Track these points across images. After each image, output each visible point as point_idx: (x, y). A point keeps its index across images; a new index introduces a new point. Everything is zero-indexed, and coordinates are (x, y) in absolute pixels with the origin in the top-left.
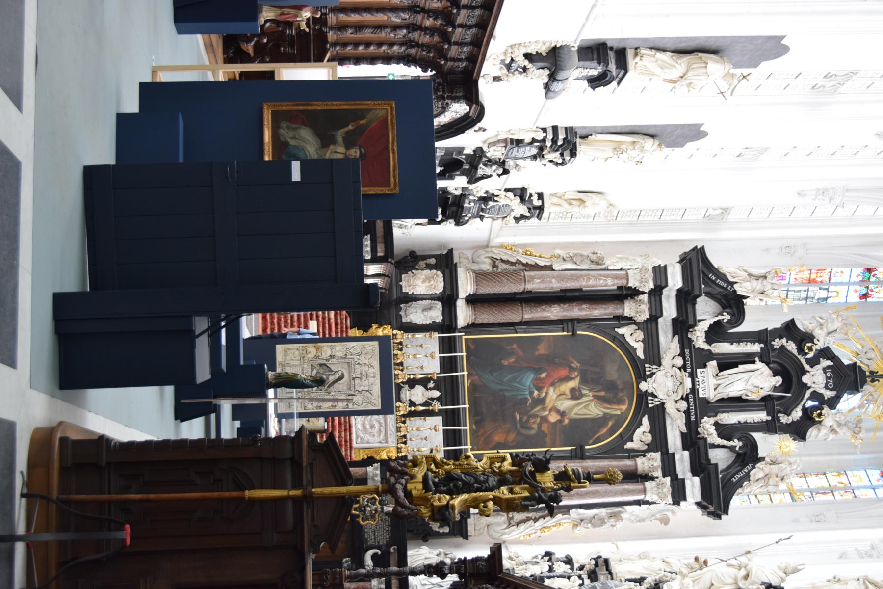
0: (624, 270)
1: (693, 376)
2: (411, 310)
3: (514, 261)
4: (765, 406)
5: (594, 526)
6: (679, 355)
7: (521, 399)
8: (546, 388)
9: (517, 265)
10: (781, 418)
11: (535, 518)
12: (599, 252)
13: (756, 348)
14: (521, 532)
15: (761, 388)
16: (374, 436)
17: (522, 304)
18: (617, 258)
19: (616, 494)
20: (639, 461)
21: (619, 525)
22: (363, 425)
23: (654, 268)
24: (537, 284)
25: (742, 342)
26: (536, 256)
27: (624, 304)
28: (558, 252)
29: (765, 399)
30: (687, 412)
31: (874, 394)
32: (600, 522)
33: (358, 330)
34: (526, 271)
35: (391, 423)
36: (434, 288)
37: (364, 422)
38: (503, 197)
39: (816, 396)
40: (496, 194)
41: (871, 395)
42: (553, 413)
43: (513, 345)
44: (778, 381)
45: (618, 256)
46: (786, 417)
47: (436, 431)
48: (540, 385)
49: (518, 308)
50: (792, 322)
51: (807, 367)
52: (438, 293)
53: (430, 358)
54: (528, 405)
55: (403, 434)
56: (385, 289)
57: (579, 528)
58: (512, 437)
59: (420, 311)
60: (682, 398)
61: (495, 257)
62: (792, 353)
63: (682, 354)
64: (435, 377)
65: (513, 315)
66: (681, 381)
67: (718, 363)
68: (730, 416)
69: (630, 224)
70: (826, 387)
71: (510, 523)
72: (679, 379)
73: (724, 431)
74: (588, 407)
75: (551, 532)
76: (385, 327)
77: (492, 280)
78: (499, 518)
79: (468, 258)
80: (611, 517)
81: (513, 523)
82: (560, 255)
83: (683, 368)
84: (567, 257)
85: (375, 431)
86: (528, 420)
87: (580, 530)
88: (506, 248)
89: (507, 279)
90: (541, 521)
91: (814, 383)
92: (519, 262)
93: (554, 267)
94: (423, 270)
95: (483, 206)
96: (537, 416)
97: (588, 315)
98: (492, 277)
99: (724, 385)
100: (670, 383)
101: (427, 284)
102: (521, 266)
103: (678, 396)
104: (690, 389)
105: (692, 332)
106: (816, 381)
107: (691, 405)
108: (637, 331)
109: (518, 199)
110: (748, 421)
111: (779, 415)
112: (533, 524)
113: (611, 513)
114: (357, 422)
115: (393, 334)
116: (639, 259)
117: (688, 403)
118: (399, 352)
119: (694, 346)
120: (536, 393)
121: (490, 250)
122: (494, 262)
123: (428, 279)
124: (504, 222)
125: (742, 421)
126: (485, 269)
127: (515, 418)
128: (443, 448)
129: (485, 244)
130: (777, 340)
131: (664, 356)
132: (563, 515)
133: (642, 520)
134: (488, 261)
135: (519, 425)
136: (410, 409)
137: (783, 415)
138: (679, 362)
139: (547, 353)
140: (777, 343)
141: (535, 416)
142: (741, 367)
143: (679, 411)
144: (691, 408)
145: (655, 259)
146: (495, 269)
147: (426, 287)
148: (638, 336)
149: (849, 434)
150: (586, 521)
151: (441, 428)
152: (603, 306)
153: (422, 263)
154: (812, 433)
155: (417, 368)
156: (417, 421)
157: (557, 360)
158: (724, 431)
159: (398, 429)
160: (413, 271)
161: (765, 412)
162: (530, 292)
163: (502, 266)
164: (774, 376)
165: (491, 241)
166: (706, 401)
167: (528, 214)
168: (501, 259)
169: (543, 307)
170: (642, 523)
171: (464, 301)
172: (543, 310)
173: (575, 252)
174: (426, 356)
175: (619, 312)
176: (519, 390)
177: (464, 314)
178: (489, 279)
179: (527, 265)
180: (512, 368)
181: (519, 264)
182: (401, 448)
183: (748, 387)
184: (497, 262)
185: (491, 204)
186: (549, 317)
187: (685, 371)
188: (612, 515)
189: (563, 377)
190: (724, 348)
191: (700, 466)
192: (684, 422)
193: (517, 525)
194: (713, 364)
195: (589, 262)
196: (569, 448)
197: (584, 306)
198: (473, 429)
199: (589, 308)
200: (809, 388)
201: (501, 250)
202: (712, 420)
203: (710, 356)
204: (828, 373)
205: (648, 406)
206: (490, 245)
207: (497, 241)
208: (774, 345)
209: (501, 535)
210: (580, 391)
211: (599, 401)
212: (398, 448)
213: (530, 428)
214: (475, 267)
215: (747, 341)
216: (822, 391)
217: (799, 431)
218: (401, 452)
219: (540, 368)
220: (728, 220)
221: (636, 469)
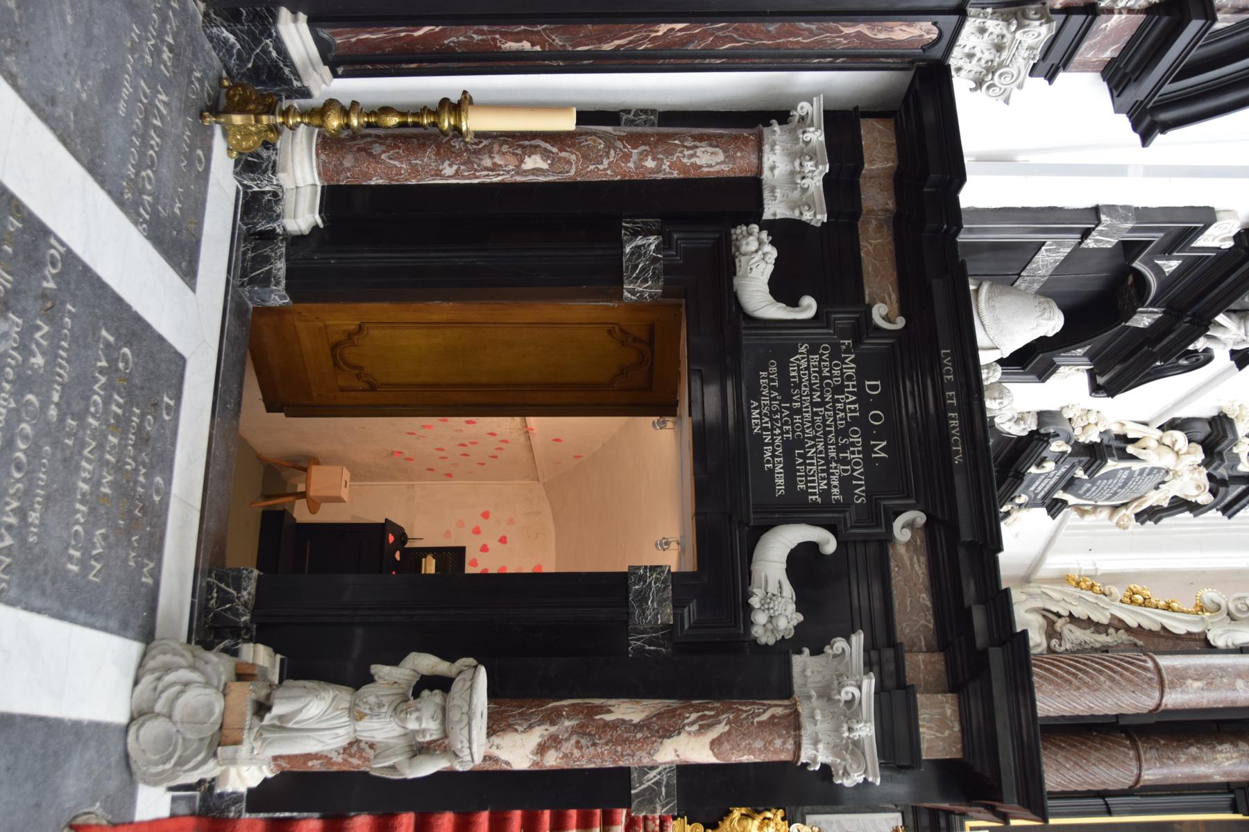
3: (1105, 621)
9: (1111, 630)
17: (1134, 743)
26: (1157, 608)
28: (1209, 595)
33: (690, 823)
38: (1153, 444)
40: (1130, 436)
49: (1126, 755)
61: (1054, 609)
65: (1114, 773)
76: (769, 815)
77: (1071, 683)
82: (1219, 608)
84: (1239, 611)
88: (1078, 584)
89: (1112, 679)
95: (1080, 473)
98: (1068, 672)
102: (1123, 636)
109: (1199, 456)
121: (1038, 591)
122: (1051, 624)
124: (1116, 519)
129: (1022, 572)
146: (1054, 642)
162: (1168, 712)
163: (1074, 636)
167: (1205, 498)
168: (1071, 615)
169: (1193, 750)
172: (1195, 759)
179: (1139, 631)
181: (1117, 630)
184: (1059, 623)
185: (1111, 465)
186: (1210, 776)
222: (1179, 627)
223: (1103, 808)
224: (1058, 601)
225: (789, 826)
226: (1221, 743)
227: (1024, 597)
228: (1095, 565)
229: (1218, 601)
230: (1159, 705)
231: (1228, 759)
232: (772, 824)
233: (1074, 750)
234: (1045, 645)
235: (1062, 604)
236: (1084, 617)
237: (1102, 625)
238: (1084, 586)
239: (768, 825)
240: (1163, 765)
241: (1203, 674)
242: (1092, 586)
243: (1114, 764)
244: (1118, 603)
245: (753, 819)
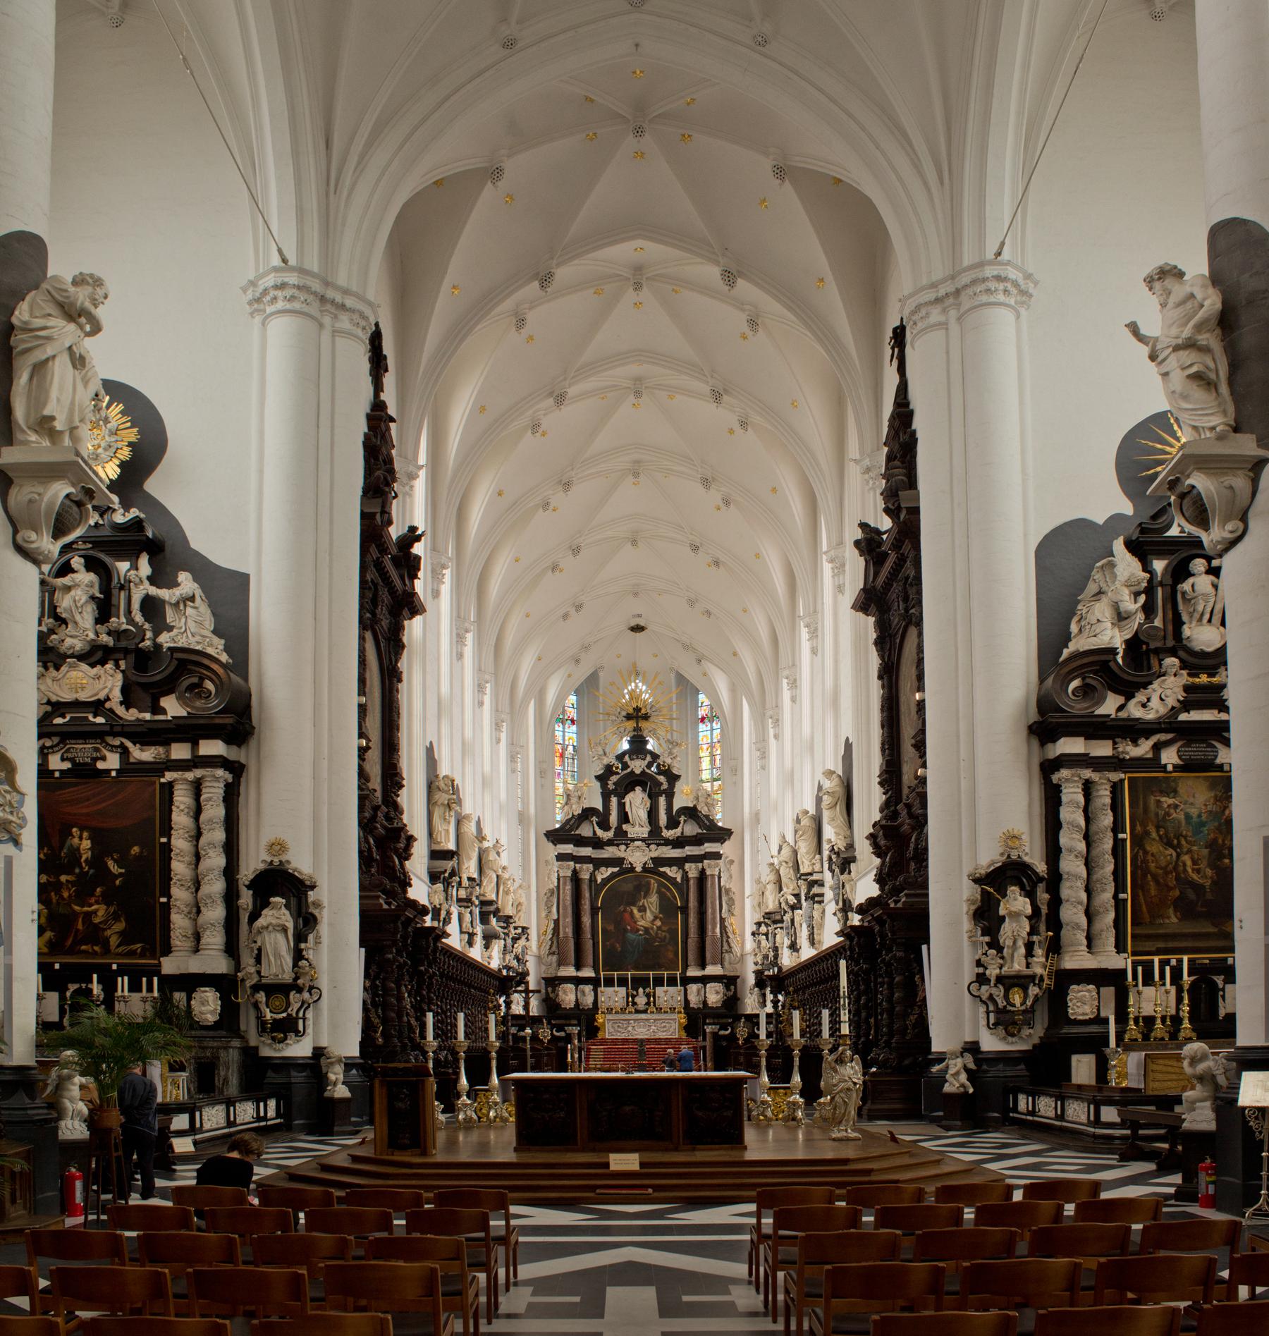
1: (633, 840)
13: (614, 800)
19: (714, 892)
20: (690, 875)
21: (734, 889)
23: (558, 860)
24: (567, 930)
29: (650, 796)
30: (658, 845)
34: (558, 935)
39: (649, 766)
44: (638, 789)
50: (598, 778)
51: (629, 770)
63: (618, 845)
70: (644, 759)
73: (673, 823)
83: (627, 845)
90: (729, 934)
92: (551, 939)
100: (638, 854)
123: (565, 993)
133: (731, 876)
138: (623, 847)
140: (611, 786)
142: (628, 809)
149: (677, 748)
151: (665, 988)
153: (551, 995)
154: (675, 771)
156: (660, 1003)
158: (673, 823)
166: (650, 833)
179: (553, 934)
190: (613, 819)
191: (697, 841)
194: (624, 827)
203: (619, 829)
214: (555, 965)
216: (646, 762)
217: (673, 778)
222: (552, 926)
241: (565, 928)
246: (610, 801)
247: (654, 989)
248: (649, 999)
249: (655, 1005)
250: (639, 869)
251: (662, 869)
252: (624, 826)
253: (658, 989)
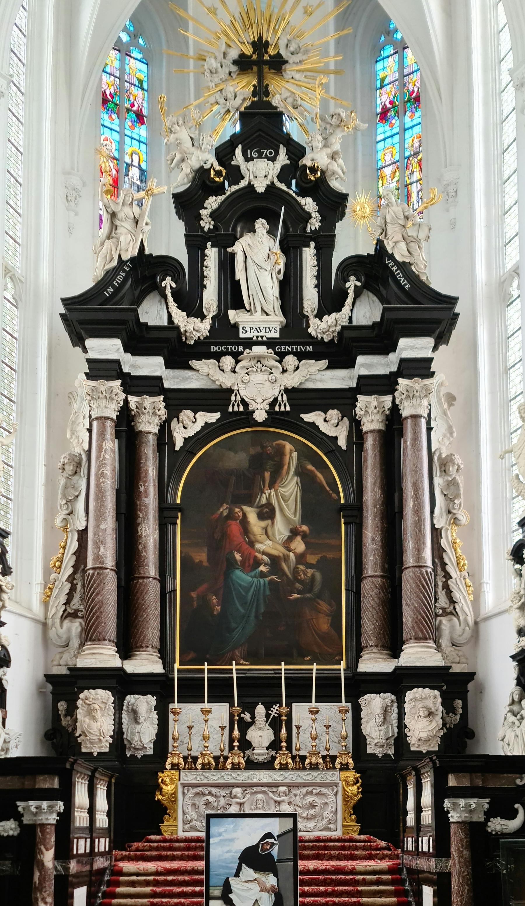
0: (91, 425)
1: (249, 344)
2: (136, 742)
3: (69, 585)
4: (295, 248)
5: (458, 496)
6: (219, 362)
7: (270, 590)
8: (257, 554)
9: (75, 582)
10: (313, 229)
11: (444, 577)
12: (62, 460)
14: (464, 597)
15: (270, 250)
16: (326, 804)
18: (71, 438)
21: (458, 459)
22: (307, 818)
25: (202, 272)
26: (64, 554)
27: (141, 432)
28: (58, 522)
29: (285, 248)
30: (301, 356)
31: (284, 96)
32: (452, 487)
34: (86, 566)
35: (305, 777)
36: (106, 703)
37: (304, 818)
41: (286, 99)
42: (293, 546)
43: (192, 597)
45: (68, 436)
46: (313, 221)
47: (317, 712)
48: (251, 561)
49: (141, 584)
52: (113, 698)
53: (210, 716)
54: (280, 580)
55: (321, 761)
56: (110, 779)
57: (460, 517)
58: (324, 606)
59: (138, 728)
60: (280, 362)
61: (61, 613)
62: (222, 203)
63: (218, 357)
64: (238, 709)
66: (256, 361)
67: (232, 308)
68: (307, 298)
69: (21, 414)
71: (451, 613)
72: (253, 363)
74: (285, 496)
75: (464, 556)
76: (160, 780)
78: (443, 627)
79: (61, 653)
80: (445, 471)
81: (452, 608)
82: (64, 519)
83: (236, 356)
84: (67, 509)
85: (319, 801)
86: (301, 582)
87: (463, 517)
88: (49, 596)
90: (450, 568)
91: (265, 176)
92: (71, 579)
93: (81, 526)
94: (77, 719)
96: (295, 568)
97: (154, 485)
99: (263, 301)
100: (259, 378)
101: (99, 714)
102: (78, 576)
103: (277, 367)
104: (268, 349)
105: (186, 339)
106: (263, 173)
107: (290, 350)
108: (181, 418)
110: (316, 274)
111: (309, 230)
112: (453, 580)
113: (440, 471)
114: (305, 829)
115: (171, 769)
116: (75, 406)
117: (288, 353)
118: (200, 761)
119: (207, 338)
120: (262, 568)
121: (51, 620)
122: (69, 615)
125: (315, 282)
126: (79, 629)
127: (297, 599)
128: (344, 704)
130: (202, 223)
131: (218, 383)
132: (442, 538)
134: (67, 623)
135: (308, 595)
136: (284, 749)
137: (308, 224)
138: (228, 361)
139: (206, 549)
140: (207, 224)
141: (295, 571)
142: (240, 275)
143: (298, 368)
144: (295, 350)
145: (76, 383)
147: (103, 715)
148: (188, 417)
150: (451, 506)
152: (143, 461)
153: (65, 722)
155: (222, 735)
157: (217, 536)
159: (314, 767)
160: (77, 734)
161: (304, 249)
164: (254, 231)
165: (38, 618)
168: (65, 604)
169: (140, 547)
170: (454, 430)
171: (125, 662)
172: (145, 547)
173: (60, 496)
174: (206, 721)
175: (152, 440)
176: (257, 592)
177: (145, 662)
178: (95, 621)
179: (75, 568)
180: (225, 601)
181: (74, 579)
182: (341, 764)
183: (269, 268)
184: (69, 610)
186: (155, 540)
187: (242, 353)
188: (443, 469)
189: (241, 528)
192: (314, 361)
193: (454, 602)
194: (233, 315)
195: (76, 478)
196: (343, 527)
197: (142, 489)
198: (310, 660)
199: (145, 482)
200: (273, 183)
201: (51, 604)
202: (314, 322)
204: (254, 155)
205: (288, 412)
206: (43, 620)
207: (37, 609)
208: (209, 228)
209: (468, 625)
210: (263, 506)
211: (278, 481)
212: (341, 769)
213: (313, 576)
214: (75, 643)
215: (202, 265)
218: (347, 764)
219: (228, 560)
220: (24, 275)
221: (379, 431)
222: (74, 546)
223: (172, 594)
224: (57, 610)
225: (167, 769)
226: (138, 532)
227: (54, 629)
228: (38, 584)
229: (61, 519)
230: (112, 570)
231: (146, 530)
232: (165, 779)
233: (137, 611)
234: (80, 620)
235: (59, 608)
236: (66, 597)
237: (71, 586)
238: (50, 593)
239: (165, 781)
240: (147, 565)
242: (49, 588)
243: (145, 591)
244: (60, 576)
245: (162, 788)
246: (204, 256)
247: (289, 705)
248: (277, 732)
249: (289, 748)
250: (260, 416)
251: (308, 417)
252: (232, 313)
253: (295, 706)
